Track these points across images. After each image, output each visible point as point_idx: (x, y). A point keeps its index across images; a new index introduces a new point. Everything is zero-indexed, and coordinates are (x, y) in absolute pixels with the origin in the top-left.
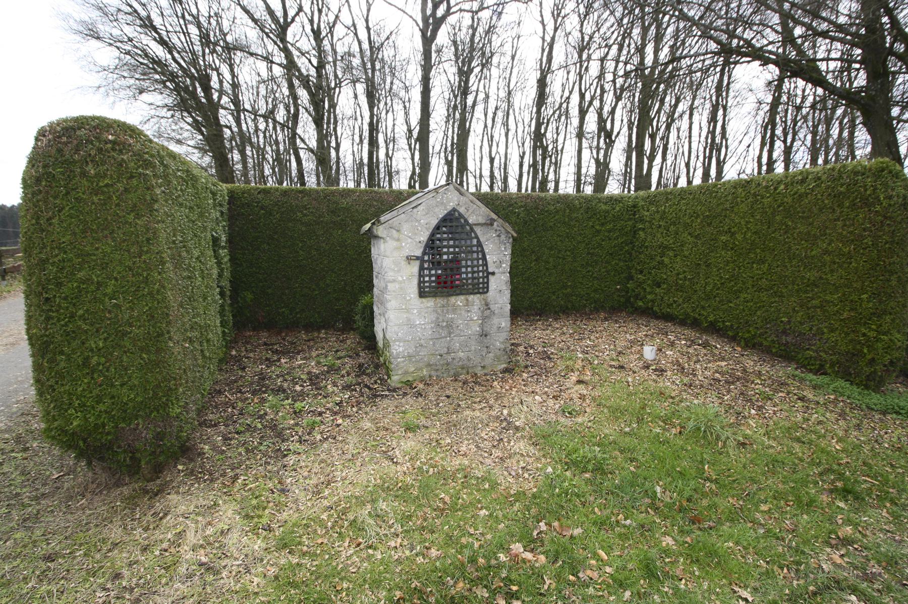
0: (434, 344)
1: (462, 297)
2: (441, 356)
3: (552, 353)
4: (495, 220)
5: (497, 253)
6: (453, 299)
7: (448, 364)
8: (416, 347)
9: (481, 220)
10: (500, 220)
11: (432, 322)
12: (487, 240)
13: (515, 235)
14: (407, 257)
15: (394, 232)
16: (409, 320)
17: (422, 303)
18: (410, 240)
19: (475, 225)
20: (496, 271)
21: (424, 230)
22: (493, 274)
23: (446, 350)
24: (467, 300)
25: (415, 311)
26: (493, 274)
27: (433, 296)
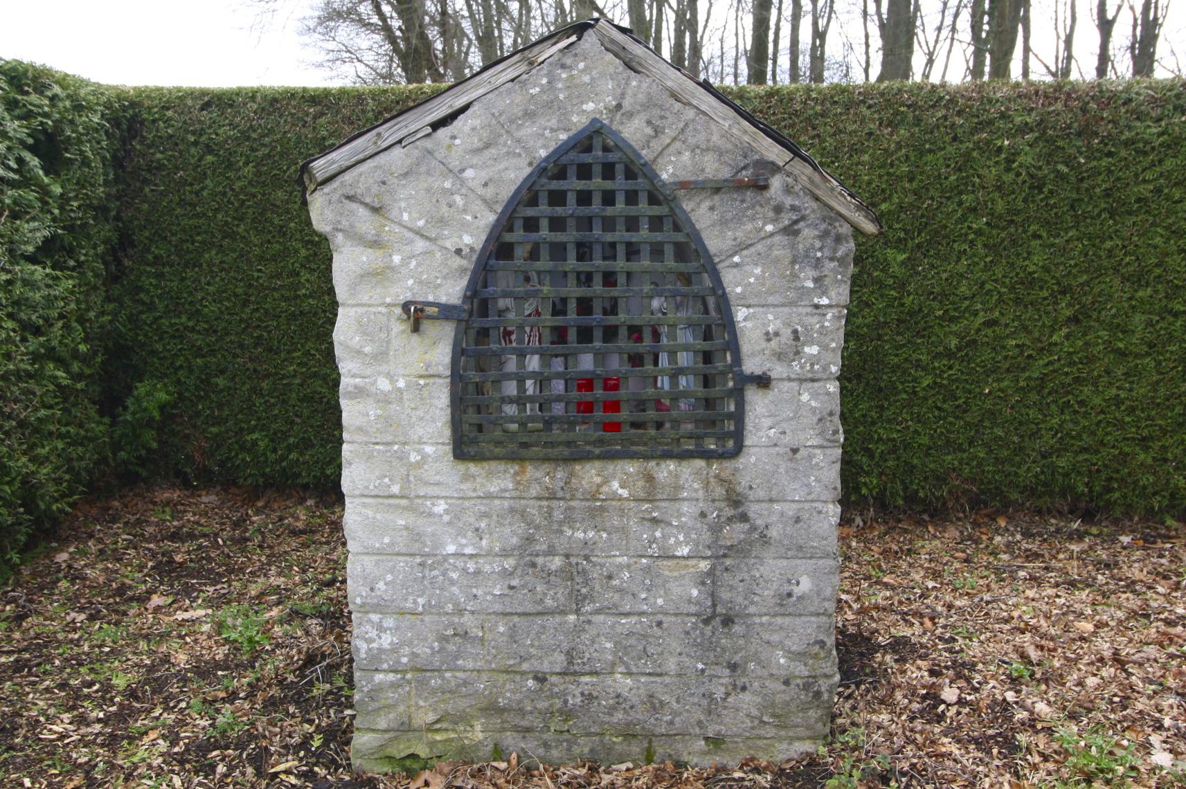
0: (513, 635)
1: (631, 467)
2: (541, 679)
3: (1031, 724)
4: (774, 168)
5: (785, 309)
6: (589, 474)
8: (444, 639)
9: (713, 168)
10: (799, 167)
11: (505, 554)
12: (741, 248)
13: (870, 227)
14: (406, 306)
15: (362, 211)
16: (416, 536)
17: (466, 477)
18: (420, 245)
19: (684, 185)
20: (778, 370)
21: (478, 206)
22: (763, 382)
23: (560, 660)
24: (650, 479)
25: (441, 507)
26: (763, 382)
27: (512, 458)
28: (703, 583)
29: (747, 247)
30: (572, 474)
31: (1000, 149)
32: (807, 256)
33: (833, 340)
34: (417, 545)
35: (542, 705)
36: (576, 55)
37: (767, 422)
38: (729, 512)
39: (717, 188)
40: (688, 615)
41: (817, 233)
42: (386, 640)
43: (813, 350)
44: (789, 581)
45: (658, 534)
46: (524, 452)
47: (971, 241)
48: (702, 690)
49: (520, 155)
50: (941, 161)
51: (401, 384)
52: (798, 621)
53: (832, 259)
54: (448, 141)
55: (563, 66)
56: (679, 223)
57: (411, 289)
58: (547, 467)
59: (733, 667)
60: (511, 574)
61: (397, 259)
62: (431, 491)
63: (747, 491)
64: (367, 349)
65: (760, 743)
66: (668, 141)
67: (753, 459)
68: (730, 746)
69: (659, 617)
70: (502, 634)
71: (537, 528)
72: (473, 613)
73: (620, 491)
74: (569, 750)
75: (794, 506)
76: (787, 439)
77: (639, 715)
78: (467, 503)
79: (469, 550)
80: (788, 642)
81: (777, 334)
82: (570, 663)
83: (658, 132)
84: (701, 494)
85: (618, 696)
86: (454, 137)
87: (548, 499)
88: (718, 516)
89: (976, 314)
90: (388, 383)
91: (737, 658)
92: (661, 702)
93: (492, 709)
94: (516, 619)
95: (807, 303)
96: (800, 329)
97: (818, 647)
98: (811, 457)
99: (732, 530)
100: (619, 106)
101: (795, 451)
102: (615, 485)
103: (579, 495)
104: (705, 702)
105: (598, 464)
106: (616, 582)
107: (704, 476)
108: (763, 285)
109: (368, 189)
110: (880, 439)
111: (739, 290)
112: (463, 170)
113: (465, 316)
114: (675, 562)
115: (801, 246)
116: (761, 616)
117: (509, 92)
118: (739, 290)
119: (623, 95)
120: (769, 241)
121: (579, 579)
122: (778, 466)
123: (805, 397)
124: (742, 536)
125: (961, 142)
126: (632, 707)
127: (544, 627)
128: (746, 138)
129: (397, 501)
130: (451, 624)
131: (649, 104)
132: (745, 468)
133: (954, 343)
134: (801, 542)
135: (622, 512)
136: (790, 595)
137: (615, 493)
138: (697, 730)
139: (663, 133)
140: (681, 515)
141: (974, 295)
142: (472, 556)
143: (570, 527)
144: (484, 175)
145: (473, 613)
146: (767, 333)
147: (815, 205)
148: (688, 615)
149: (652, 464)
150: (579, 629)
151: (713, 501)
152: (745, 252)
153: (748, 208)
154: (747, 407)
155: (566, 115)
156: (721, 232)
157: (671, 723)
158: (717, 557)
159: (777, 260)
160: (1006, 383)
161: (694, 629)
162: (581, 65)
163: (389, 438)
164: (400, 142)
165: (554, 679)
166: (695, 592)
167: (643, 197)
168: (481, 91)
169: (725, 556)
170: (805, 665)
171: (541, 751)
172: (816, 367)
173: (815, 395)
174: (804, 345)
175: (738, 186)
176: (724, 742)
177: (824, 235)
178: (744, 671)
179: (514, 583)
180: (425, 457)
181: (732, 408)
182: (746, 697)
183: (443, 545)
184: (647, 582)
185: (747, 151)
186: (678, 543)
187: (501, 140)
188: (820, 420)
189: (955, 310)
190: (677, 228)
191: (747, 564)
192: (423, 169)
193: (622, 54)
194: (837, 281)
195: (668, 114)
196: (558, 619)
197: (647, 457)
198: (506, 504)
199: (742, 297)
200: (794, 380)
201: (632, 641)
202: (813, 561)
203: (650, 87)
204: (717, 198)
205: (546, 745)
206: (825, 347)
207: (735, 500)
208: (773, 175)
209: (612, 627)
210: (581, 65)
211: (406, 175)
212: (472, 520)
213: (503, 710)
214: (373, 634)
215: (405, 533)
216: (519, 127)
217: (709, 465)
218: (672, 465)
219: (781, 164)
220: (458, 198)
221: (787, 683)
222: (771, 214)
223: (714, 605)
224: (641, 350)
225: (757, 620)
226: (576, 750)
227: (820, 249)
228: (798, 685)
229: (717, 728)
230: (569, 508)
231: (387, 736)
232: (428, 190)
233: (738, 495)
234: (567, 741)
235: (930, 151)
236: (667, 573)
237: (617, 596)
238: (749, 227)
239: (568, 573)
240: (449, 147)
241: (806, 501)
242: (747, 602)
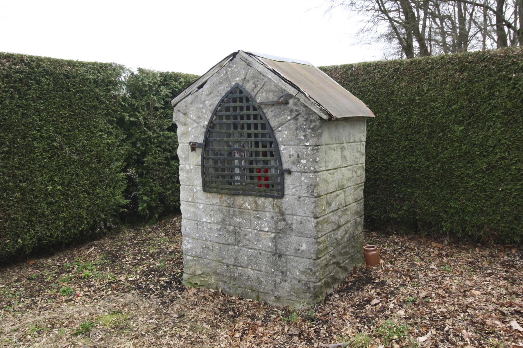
1: (251, 199)
2: (228, 266)
6: (239, 200)
7: (235, 279)
8: (203, 248)
9: (272, 97)
12: (281, 125)
15: (181, 115)
16: (196, 215)
18: (195, 125)
20: (294, 168)
22: (289, 172)
24: (256, 203)
25: (201, 206)
26: (289, 172)
27: (219, 193)
28: (273, 241)
30: (235, 200)
31: (510, 79)
33: (311, 158)
35: (229, 275)
38: (280, 217)
39: (273, 104)
40: (269, 252)
42: (189, 246)
44: (299, 245)
45: (259, 222)
47: (495, 121)
48: (273, 279)
50: (482, 85)
51: (192, 167)
52: (303, 260)
53: (309, 129)
55: (230, 67)
58: (228, 196)
59: (283, 273)
60: (220, 230)
61: (190, 129)
62: (200, 201)
64: (183, 156)
65: (291, 302)
67: (287, 199)
69: (261, 251)
71: (226, 216)
73: (248, 207)
74: (235, 291)
75: (300, 217)
76: (297, 193)
77: (255, 283)
78: (208, 206)
79: (209, 221)
80: (299, 267)
81: (293, 155)
82: (235, 262)
83: (256, 86)
84: (272, 210)
86: (203, 91)
89: (496, 154)
90: (190, 168)
91: (284, 270)
93: (216, 273)
94: (221, 245)
98: (304, 200)
99: (280, 224)
100: (245, 78)
101: (300, 198)
102: (247, 204)
105: (242, 197)
106: (247, 237)
110: (451, 207)
111: (281, 139)
112: (205, 101)
113: (203, 147)
116: (291, 256)
117: (216, 76)
118: (281, 139)
119: (247, 74)
120: (289, 122)
121: (237, 235)
123: (303, 178)
125: (492, 76)
128: (283, 87)
131: (253, 77)
133: (485, 166)
135: (249, 214)
136: (299, 250)
137: (247, 207)
140: (266, 217)
141: (496, 146)
142: (210, 223)
144: (210, 102)
146: (290, 155)
147: (304, 109)
149: (257, 198)
150: (238, 252)
152: (283, 126)
154: (285, 181)
156: (275, 119)
157: (264, 288)
158: (277, 233)
159: (291, 129)
160: (510, 186)
161: (270, 257)
162: (235, 66)
163: (189, 184)
165: (231, 267)
166: (270, 244)
167: (251, 108)
168: (209, 76)
169: (279, 233)
170: (306, 276)
171: (228, 290)
174: (301, 159)
175: (282, 103)
177: (306, 120)
178: (286, 274)
179: (220, 233)
180: (197, 190)
181: (279, 181)
182: (286, 284)
183: (202, 219)
185: (283, 91)
186: (265, 226)
188: (308, 187)
189: (486, 152)
190: (261, 118)
192: (196, 101)
194: (312, 137)
195: (259, 80)
196: (233, 247)
197: (256, 196)
198: (218, 207)
199: (282, 142)
200: (298, 172)
201: (252, 258)
202: (307, 239)
204: (273, 108)
205: (229, 288)
206: (308, 161)
207: (282, 214)
209: (247, 252)
210: (235, 66)
211: (191, 103)
213: (218, 274)
214: (186, 244)
217: (274, 200)
218: (263, 199)
219: (294, 95)
220: (204, 110)
221: (299, 282)
222: (289, 113)
223: (276, 250)
224: (252, 159)
226: (238, 292)
227: (305, 125)
230: (234, 211)
232: (197, 108)
235: (477, 81)
238: (283, 117)
239: (235, 232)
240: (202, 94)
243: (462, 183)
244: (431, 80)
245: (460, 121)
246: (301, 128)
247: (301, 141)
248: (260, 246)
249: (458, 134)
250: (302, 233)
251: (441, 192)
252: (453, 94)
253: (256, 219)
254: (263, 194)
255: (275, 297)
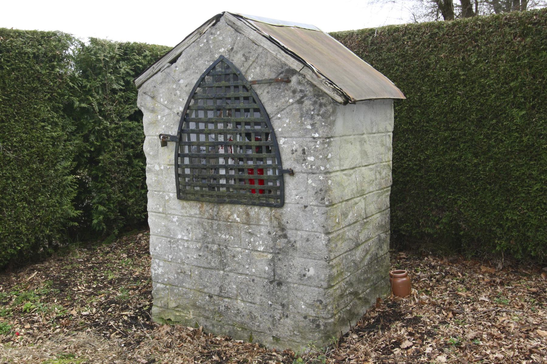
2: (211, 297)
4: (293, 72)
6: (226, 210)
7: (221, 314)
8: (178, 273)
9: (269, 74)
11: (197, 241)
12: (280, 110)
15: (149, 99)
16: (168, 230)
18: (167, 111)
20: (297, 168)
22: (291, 173)
24: (248, 214)
25: (175, 219)
26: (291, 173)
27: (197, 200)
28: (270, 265)
29: (282, 110)
30: (219, 210)
32: (307, 114)
33: (321, 154)
34: (168, 233)
35: (212, 308)
36: (216, 28)
37: (294, 192)
38: (280, 233)
40: (265, 278)
41: (311, 102)
42: (160, 271)
43: (311, 159)
44: (305, 269)
45: (252, 240)
46: (201, 199)
48: (270, 314)
49: (197, 73)
51: (162, 168)
52: (309, 289)
53: (318, 115)
54: (174, 69)
55: (212, 34)
56: (255, 99)
57: (164, 129)
58: (211, 206)
59: (283, 306)
60: (200, 250)
61: (159, 117)
63: (286, 224)
64: (151, 153)
65: (294, 344)
66: (251, 63)
67: (289, 209)
68: (283, 342)
70: (197, 275)
71: (207, 231)
72: (187, 264)
73: (237, 219)
74: (221, 329)
75: (307, 233)
76: (303, 201)
77: (246, 320)
78: (184, 218)
79: (185, 238)
80: (305, 298)
81: (296, 151)
82: (221, 292)
83: (247, 59)
84: (268, 223)
85: (238, 310)
86: (176, 67)
87: (211, 219)
88: (276, 234)
90: (160, 168)
91: (284, 302)
92: (255, 316)
93: (195, 306)
94: (202, 269)
95: (309, 136)
96: (306, 148)
97: (319, 303)
98: (312, 210)
99: (280, 242)
100: (232, 49)
101: (306, 207)
102: (235, 216)
103: (222, 219)
104: (271, 319)
106: (236, 259)
107: (269, 215)
108: (290, 127)
109: (150, 90)
110: (507, 218)
111: (280, 130)
112: (179, 80)
113: (178, 140)
114: (259, 253)
115: (304, 109)
116: (294, 284)
118: (280, 130)
119: (234, 44)
120: (291, 107)
121: (223, 256)
122: (299, 213)
123: (310, 181)
124: (284, 245)
126: (243, 316)
127: (212, 274)
128: (283, 59)
129: (162, 215)
130: (180, 268)
132: (286, 213)
134: (309, 251)
135: (238, 228)
136: (304, 275)
137: (235, 219)
138: (268, 332)
139: (249, 59)
140: (261, 232)
142: (187, 241)
143: (220, 233)
144: (186, 82)
145: (187, 264)
146: (292, 150)
147: (311, 89)
148: (265, 278)
149: (249, 208)
150: (224, 278)
151: (274, 227)
152: (283, 112)
153: (282, 92)
154: (286, 185)
155: (213, 55)
157: (259, 326)
158: (275, 253)
159: (294, 116)
161: (267, 285)
162: (218, 33)
163: (159, 189)
164: (160, 70)
165: (215, 297)
166: (267, 268)
168: (185, 47)
169: (278, 253)
170: (314, 311)
171: (211, 327)
172: (314, 167)
173: (314, 181)
174: (307, 156)
175: (282, 81)
176: (280, 340)
177: (315, 103)
178: (288, 308)
179: (201, 254)
180: (170, 198)
181: (278, 184)
182: (288, 321)
183: (177, 235)
184: (249, 261)
186: (259, 245)
187: (191, 67)
188: (316, 193)
190: (254, 101)
191: (287, 258)
192: (167, 81)
193: (234, 26)
194: (322, 126)
195: (251, 51)
196: (217, 272)
197: (246, 204)
199: (281, 133)
200: (304, 173)
201: (243, 286)
202: (316, 261)
203: (244, 40)
204: (270, 87)
205: (213, 325)
206: (317, 157)
208: (293, 76)
209: (235, 279)
210: (218, 33)
211: (161, 83)
212: (186, 225)
213: (198, 307)
214: (156, 267)
215: (164, 228)
216: (197, 61)
217: (271, 211)
218: (256, 209)
219: (298, 70)
220: (178, 92)
221: (305, 317)
222: (291, 94)
223: (274, 275)
225: (292, 285)
226: (224, 330)
227: (313, 110)
228: (310, 320)
229: (277, 332)
230: (219, 224)
231: (161, 309)
232: (168, 89)
233: (283, 225)
234: (221, 325)
236: (256, 258)
237: (237, 265)
238: (283, 100)
239: (220, 253)
240: (175, 71)
241: (312, 231)
242: (287, 276)
243: (522, 187)
244: (481, 48)
245: (521, 103)
246: (307, 114)
247: (307, 131)
248: (254, 270)
249: (518, 120)
250: (309, 254)
251: (493, 198)
252: (511, 67)
253: (248, 235)
254: (257, 201)
255: (273, 337)
